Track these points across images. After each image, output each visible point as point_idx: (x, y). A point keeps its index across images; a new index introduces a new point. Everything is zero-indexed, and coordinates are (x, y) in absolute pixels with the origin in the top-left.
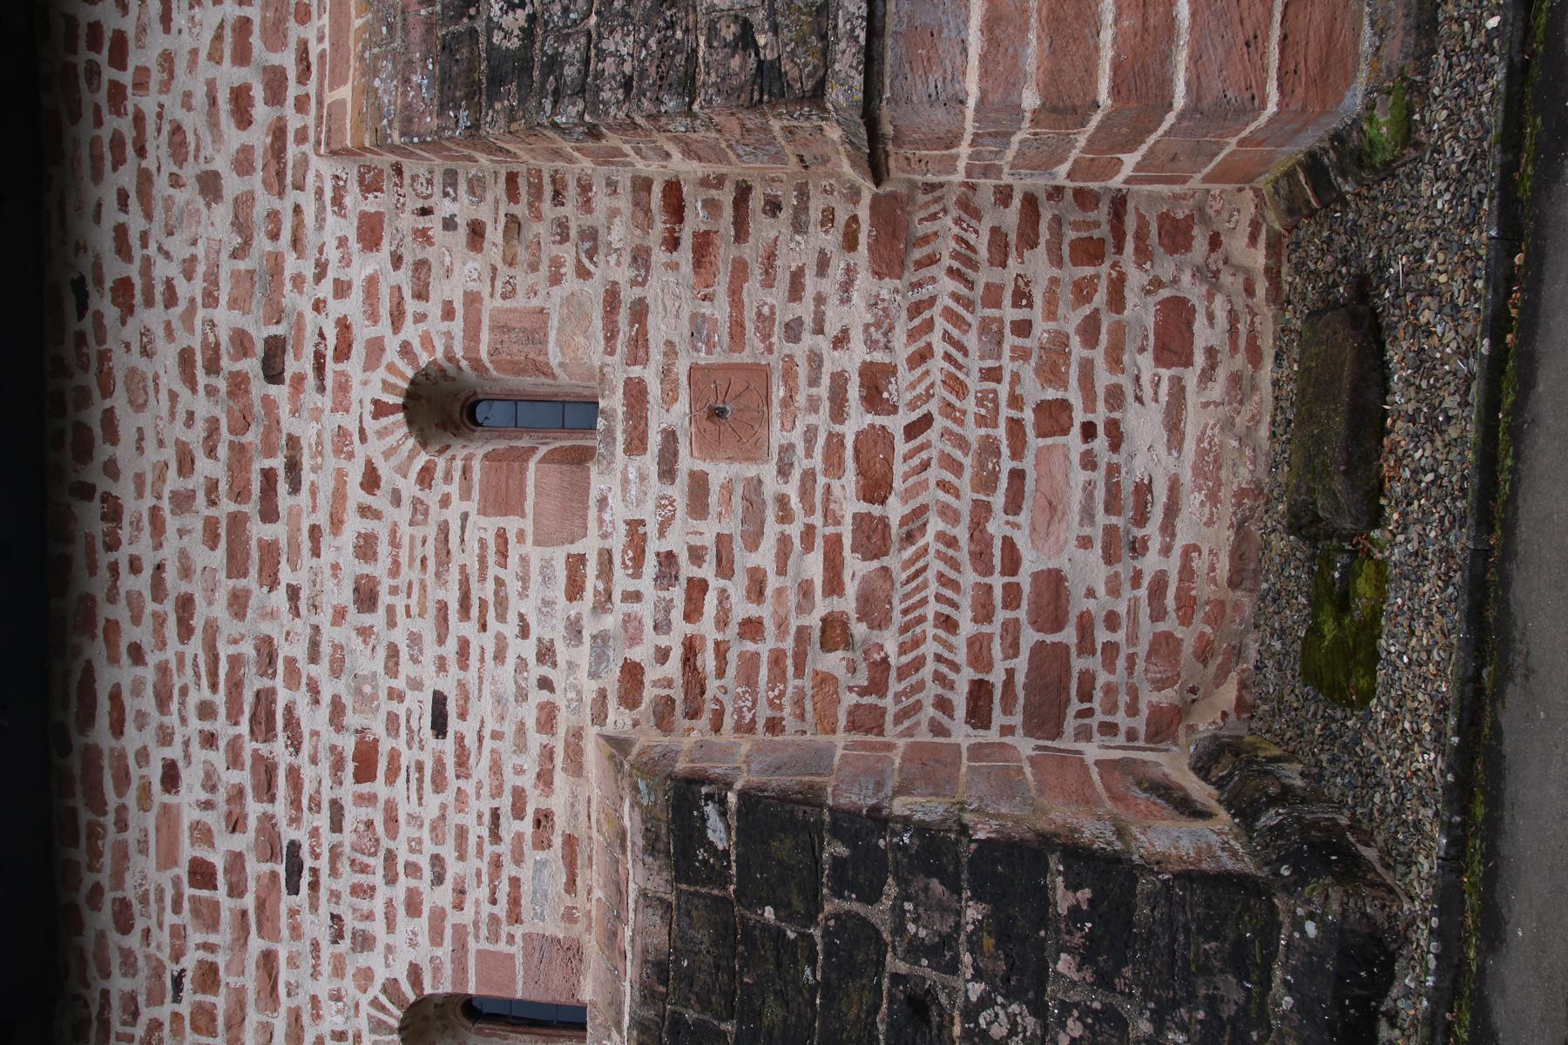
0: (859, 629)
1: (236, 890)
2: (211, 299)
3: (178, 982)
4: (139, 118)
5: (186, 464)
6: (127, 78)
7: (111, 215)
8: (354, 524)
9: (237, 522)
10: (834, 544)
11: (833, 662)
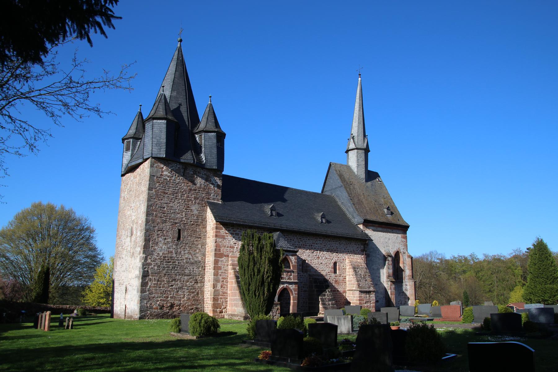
5: (332, 246)
7: (343, 243)
8: (330, 258)
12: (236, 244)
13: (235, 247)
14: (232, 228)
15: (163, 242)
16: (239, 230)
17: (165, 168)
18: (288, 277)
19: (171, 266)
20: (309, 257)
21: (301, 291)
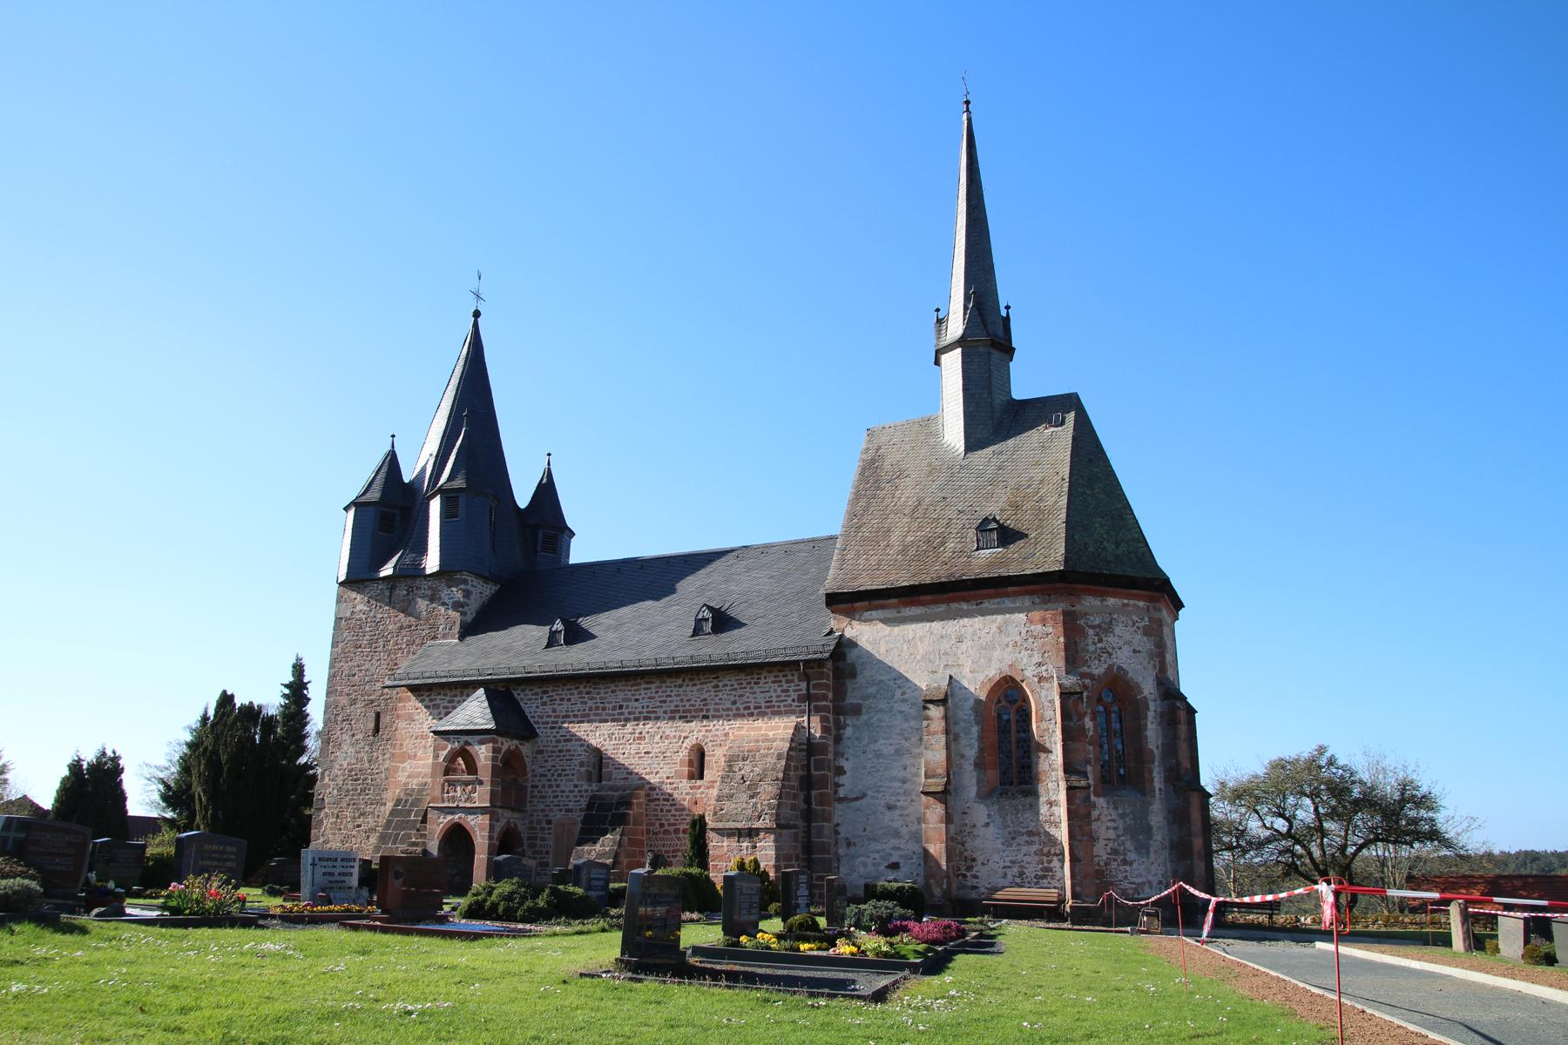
0: (662, 830)
1: (619, 714)
2: (716, 704)
3: (603, 703)
4: (745, 688)
5: (688, 700)
6: (752, 685)
7: (729, 683)
8: (678, 734)
9: (678, 711)
10: (675, 824)
11: (657, 825)
14: (427, 694)
15: (348, 742)
17: (359, 597)
18: (466, 797)
19: (359, 787)
20: (611, 740)
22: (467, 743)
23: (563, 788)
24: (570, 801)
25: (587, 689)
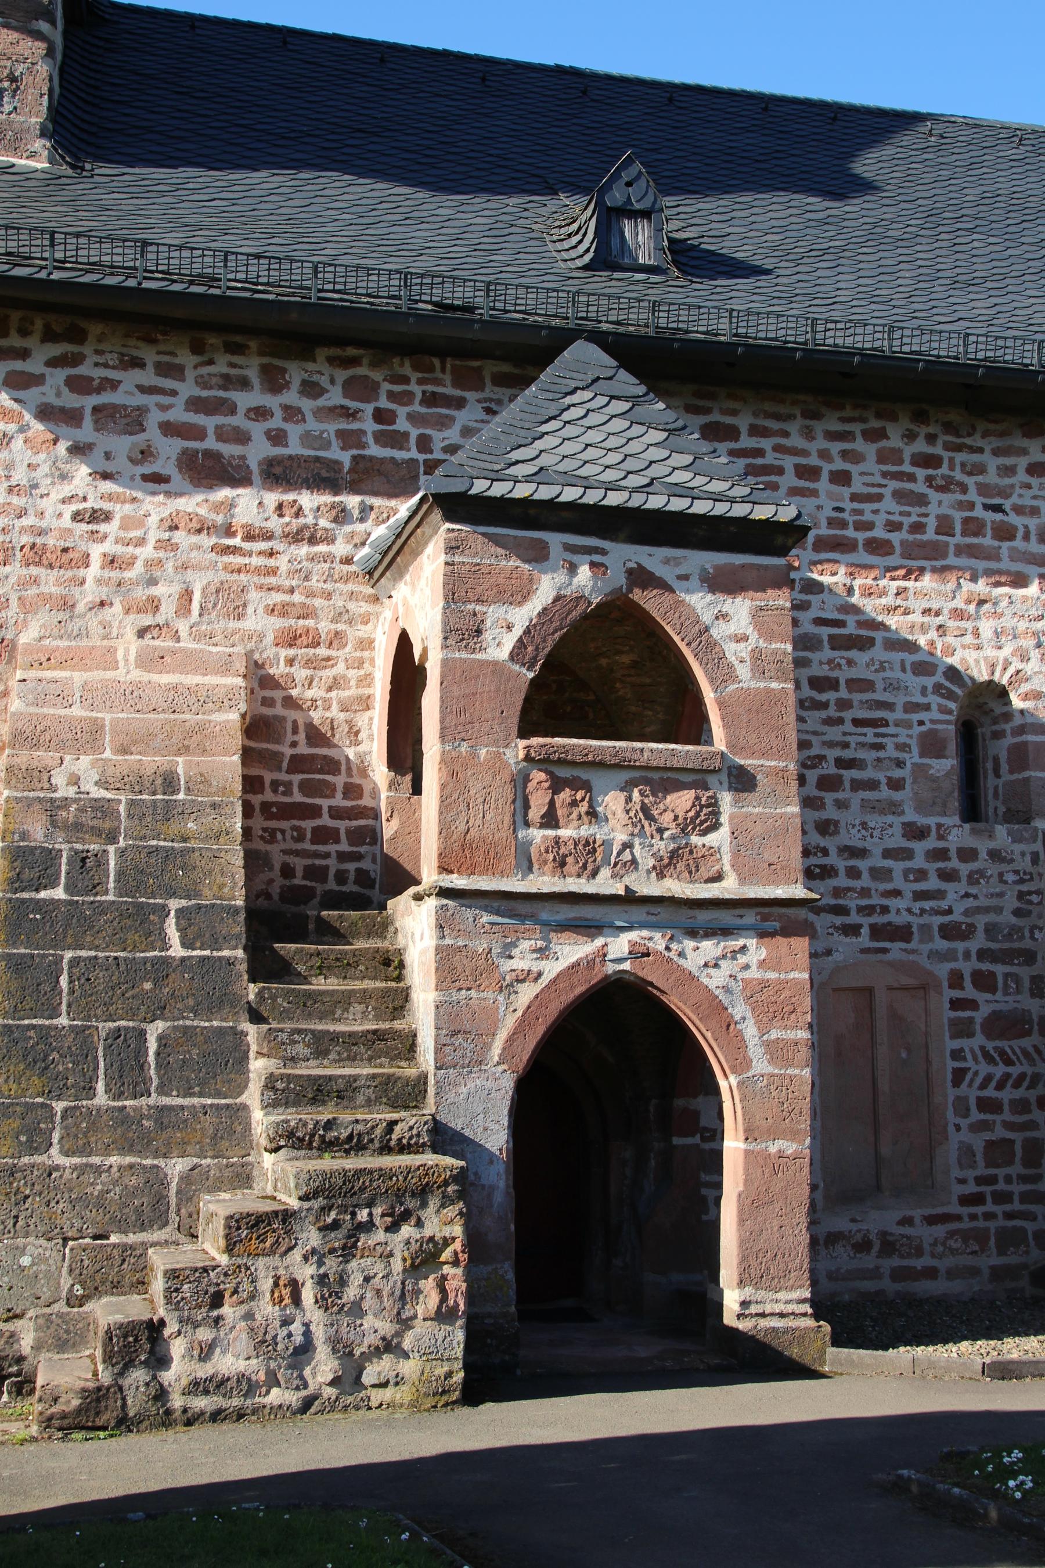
3: (998, 509)
12: (97, 516)
13: (96, 551)
16: (147, 377)
18: (663, 846)
21: (962, 1029)
22: (641, 578)
23: (853, 838)
24: (897, 893)
25: (920, 446)
